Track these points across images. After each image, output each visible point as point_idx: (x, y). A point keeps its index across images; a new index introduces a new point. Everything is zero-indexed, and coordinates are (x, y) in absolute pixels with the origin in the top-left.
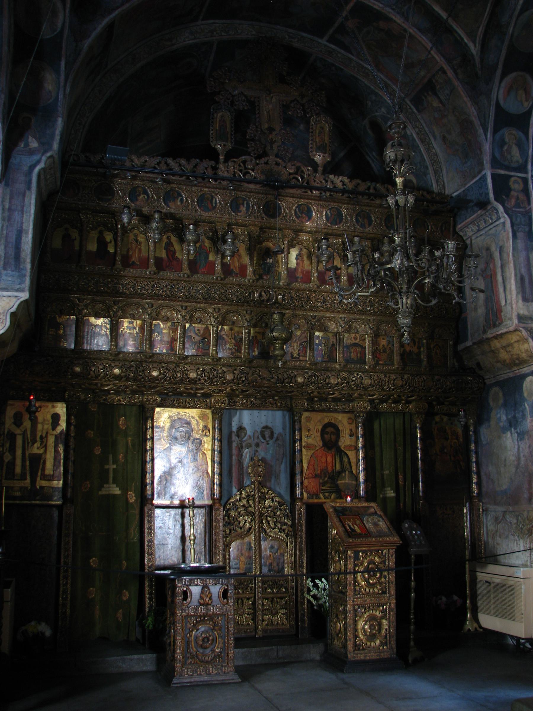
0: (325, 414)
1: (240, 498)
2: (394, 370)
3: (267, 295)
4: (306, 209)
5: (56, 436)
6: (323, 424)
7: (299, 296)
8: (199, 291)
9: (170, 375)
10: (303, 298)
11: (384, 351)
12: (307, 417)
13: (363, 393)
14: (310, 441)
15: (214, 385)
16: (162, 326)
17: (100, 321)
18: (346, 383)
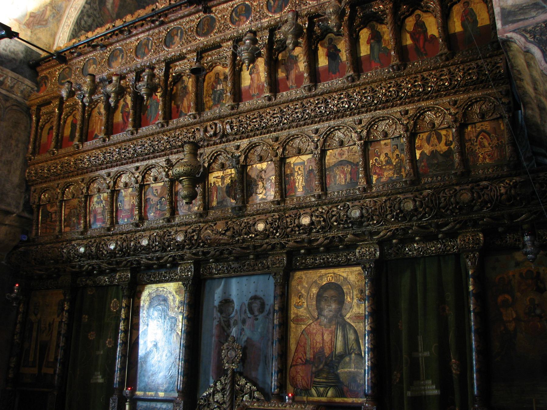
0: (323, 271)
1: (214, 391)
2: (402, 188)
3: (212, 129)
4: (244, 9)
5: (59, 322)
6: (320, 286)
7: (249, 118)
8: (144, 146)
9: (125, 244)
10: (255, 118)
11: (389, 162)
12: (299, 278)
13: (359, 231)
14: (302, 312)
15: (170, 251)
16: (124, 194)
17: (75, 202)
18: (324, 221)
